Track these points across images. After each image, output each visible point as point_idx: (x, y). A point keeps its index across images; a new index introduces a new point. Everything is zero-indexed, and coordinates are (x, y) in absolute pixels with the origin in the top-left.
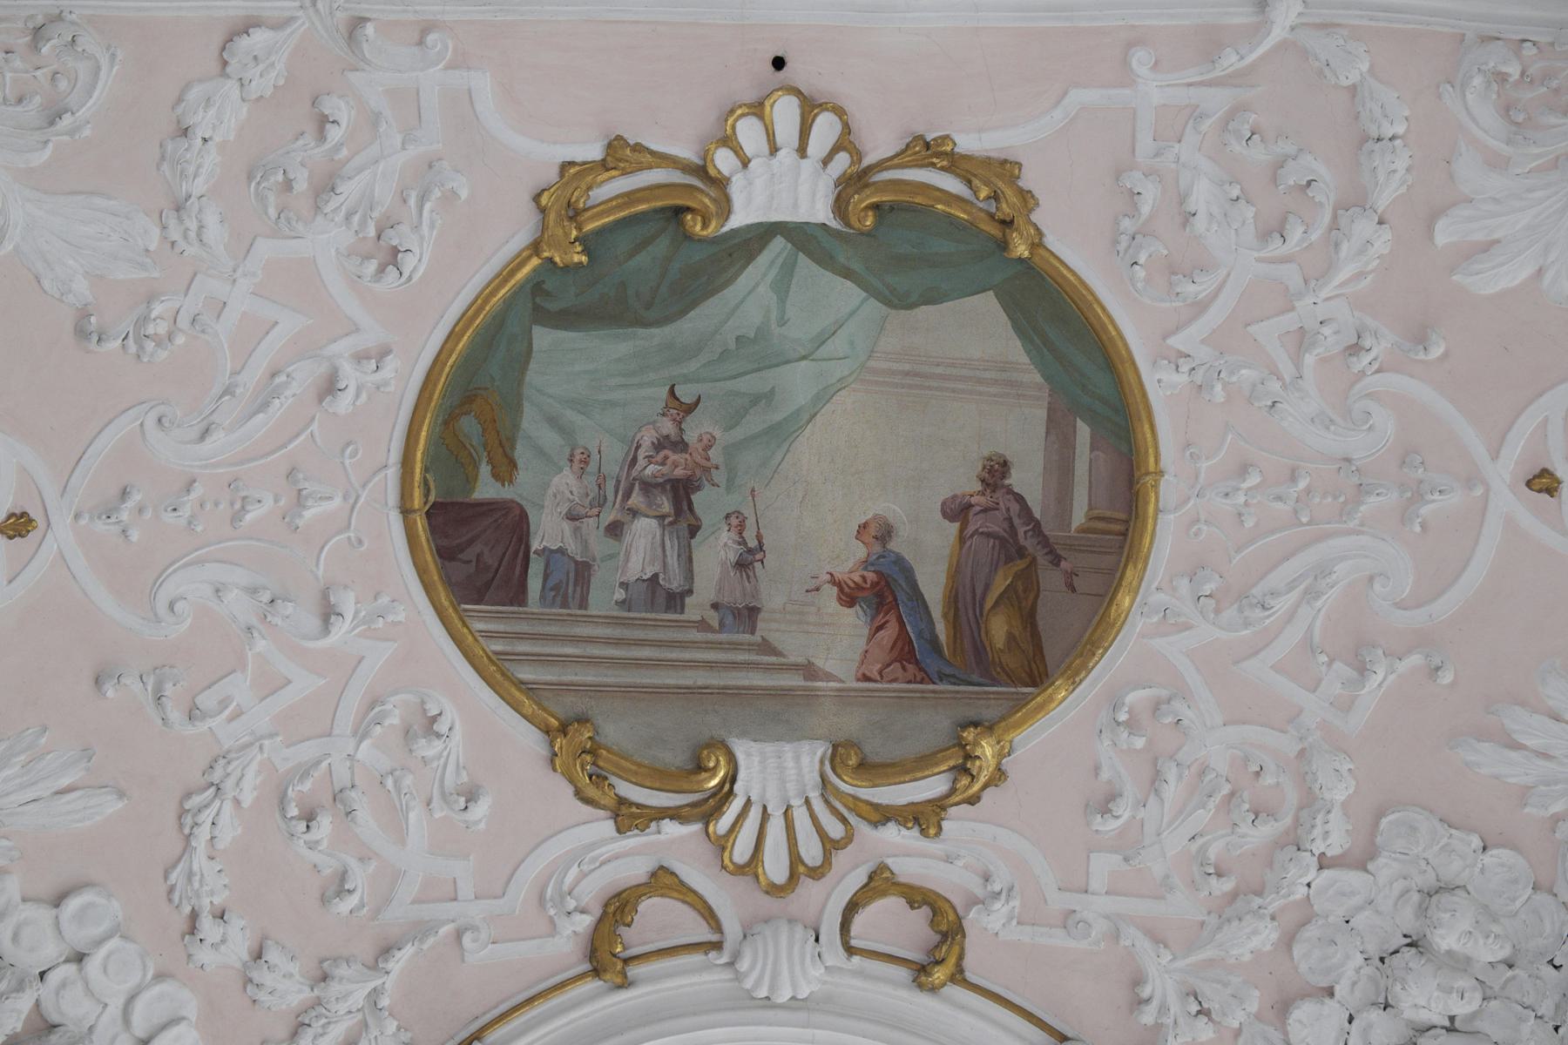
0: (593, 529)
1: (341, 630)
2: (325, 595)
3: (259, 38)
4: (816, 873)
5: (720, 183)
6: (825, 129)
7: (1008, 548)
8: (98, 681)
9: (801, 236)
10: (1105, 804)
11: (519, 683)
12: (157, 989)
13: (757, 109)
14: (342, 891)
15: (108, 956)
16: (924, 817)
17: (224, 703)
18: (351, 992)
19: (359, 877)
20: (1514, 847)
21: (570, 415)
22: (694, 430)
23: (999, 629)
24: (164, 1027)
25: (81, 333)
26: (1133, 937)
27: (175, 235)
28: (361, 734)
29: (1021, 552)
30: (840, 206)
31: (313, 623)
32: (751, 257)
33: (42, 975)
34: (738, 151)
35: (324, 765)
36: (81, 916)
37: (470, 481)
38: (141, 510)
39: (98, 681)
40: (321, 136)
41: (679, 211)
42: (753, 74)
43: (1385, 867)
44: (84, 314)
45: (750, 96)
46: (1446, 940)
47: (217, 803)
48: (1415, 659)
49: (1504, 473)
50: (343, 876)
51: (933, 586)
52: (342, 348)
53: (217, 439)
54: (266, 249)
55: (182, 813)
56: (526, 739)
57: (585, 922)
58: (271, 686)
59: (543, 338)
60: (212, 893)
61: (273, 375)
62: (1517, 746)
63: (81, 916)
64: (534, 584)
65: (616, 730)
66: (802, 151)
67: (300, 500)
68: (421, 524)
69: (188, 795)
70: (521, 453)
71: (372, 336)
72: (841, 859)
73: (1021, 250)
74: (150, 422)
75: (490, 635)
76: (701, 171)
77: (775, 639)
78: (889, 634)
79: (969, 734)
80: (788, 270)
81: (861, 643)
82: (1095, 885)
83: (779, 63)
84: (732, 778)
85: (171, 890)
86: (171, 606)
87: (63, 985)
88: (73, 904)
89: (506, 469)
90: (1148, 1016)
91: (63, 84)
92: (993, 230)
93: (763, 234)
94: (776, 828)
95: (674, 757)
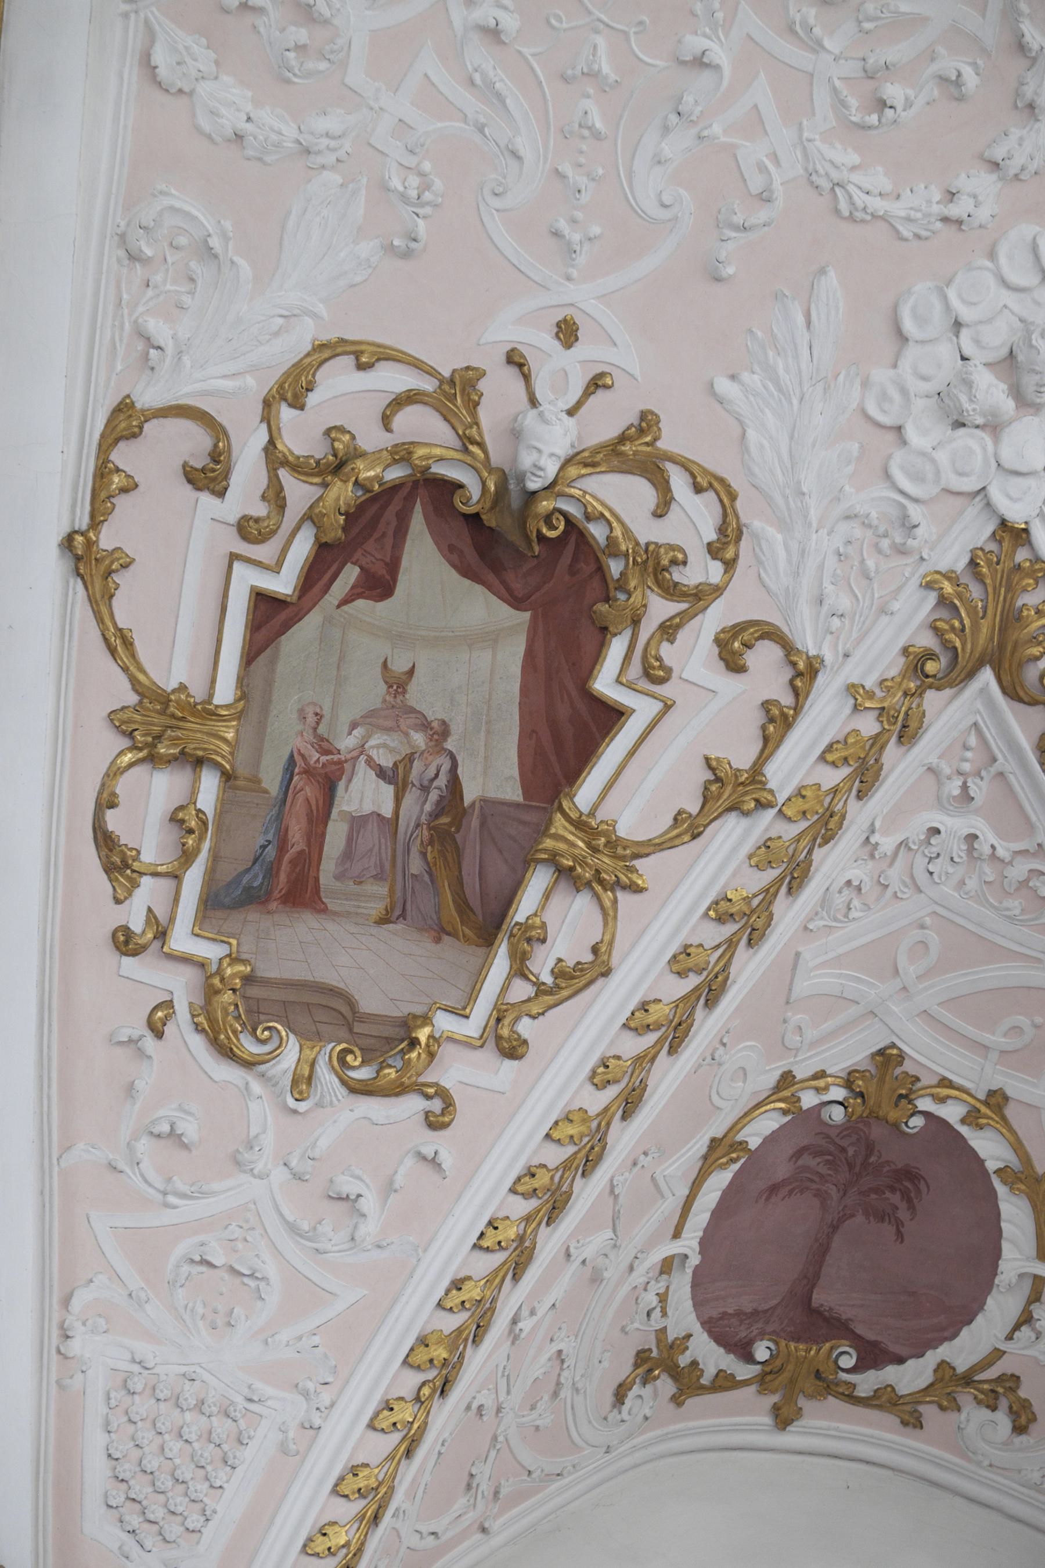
1: (719, 54)
3: (160, 57)
8: (718, 279)
12: (1003, 260)
14: (958, 82)
15: (964, 301)
17: (762, 168)
19: (948, 64)
25: (407, 254)
27: (330, 159)
28: (817, 47)
31: (706, 78)
33: (963, 358)
35: (838, 83)
36: (921, 321)
38: (574, 221)
39: (718, 279)
44: (390, 249)
47: (851, 188)
50: (943, 79)
53: (522, 145)
54: (356, 76)
55: (851, 218)
60: (929, 202)
61: (472, 83)
67: (592, 75)
69: (837, 212)
74: (496, 203)
85: (918, 236)
86: (665, 206)
87: (977, 342)
88: (909, 326)
91: (183, 241)
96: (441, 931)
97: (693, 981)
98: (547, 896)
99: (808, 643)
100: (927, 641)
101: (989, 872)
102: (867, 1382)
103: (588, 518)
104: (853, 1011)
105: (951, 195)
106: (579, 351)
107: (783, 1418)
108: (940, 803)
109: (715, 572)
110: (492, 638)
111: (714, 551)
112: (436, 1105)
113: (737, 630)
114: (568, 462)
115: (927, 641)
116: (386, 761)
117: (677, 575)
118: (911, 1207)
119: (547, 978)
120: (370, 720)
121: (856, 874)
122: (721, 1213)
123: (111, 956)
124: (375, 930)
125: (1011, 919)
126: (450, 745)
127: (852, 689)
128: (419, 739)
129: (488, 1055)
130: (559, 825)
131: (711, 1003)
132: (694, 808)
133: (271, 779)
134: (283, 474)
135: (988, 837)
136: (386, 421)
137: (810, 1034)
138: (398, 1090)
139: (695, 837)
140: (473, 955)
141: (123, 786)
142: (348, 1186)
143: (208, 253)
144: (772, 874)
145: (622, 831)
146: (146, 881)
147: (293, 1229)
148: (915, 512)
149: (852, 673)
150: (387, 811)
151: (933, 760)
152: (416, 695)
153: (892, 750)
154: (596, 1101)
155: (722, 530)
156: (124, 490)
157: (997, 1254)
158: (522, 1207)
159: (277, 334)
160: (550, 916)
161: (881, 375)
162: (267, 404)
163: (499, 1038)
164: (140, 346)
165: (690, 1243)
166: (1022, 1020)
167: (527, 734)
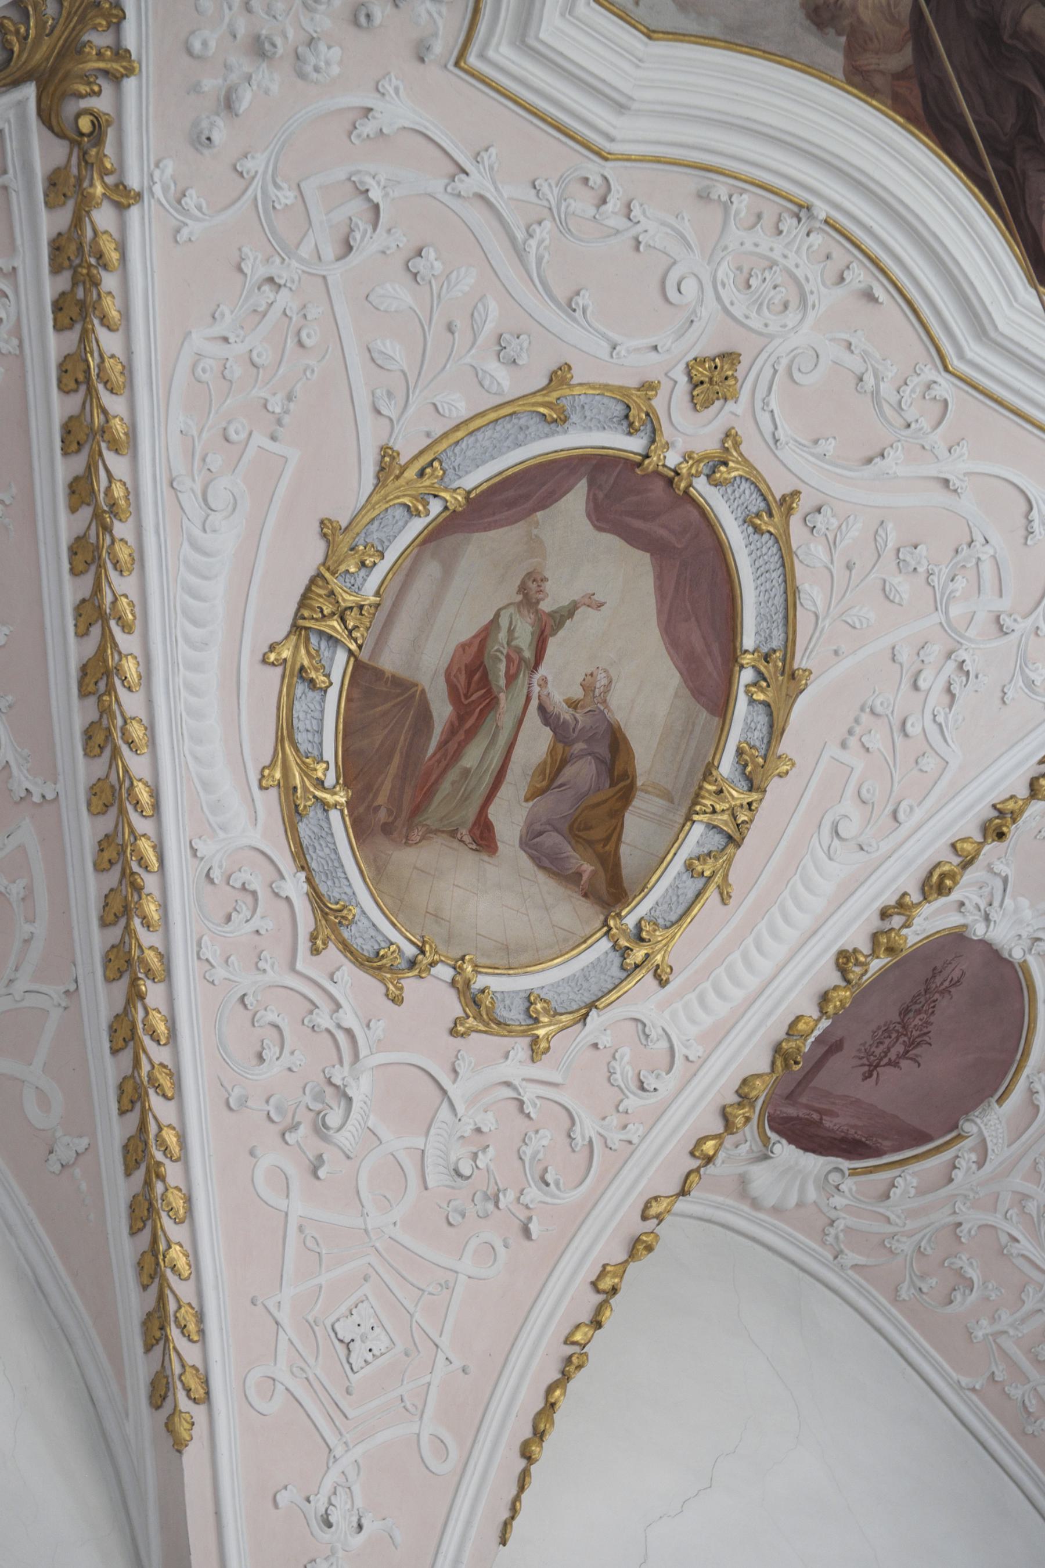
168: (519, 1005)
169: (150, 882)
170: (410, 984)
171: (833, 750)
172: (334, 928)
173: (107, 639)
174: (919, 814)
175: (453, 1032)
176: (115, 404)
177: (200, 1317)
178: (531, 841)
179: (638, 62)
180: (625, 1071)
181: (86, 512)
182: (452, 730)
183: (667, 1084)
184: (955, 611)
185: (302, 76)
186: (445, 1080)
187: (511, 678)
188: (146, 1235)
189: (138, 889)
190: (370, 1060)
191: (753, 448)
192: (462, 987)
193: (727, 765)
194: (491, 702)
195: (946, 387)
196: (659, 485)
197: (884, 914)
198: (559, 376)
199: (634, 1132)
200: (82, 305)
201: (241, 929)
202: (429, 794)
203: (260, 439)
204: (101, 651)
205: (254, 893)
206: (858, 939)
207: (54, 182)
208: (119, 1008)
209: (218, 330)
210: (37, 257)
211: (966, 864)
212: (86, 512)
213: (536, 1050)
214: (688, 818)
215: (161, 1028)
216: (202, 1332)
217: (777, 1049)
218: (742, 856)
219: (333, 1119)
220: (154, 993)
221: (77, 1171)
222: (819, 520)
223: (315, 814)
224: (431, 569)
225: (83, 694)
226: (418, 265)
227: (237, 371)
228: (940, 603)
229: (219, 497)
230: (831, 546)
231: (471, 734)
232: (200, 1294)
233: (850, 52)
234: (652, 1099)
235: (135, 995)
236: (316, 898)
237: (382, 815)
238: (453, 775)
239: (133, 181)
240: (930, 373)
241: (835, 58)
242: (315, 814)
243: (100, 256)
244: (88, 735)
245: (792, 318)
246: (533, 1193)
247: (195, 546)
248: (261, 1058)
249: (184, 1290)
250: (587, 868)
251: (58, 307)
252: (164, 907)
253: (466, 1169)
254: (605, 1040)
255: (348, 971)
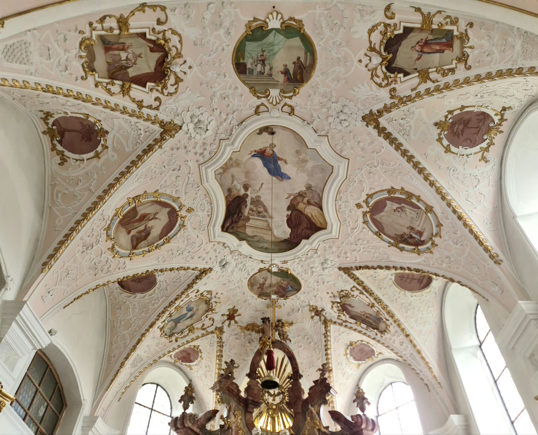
0: (254, 65)
1: (227, 78)
2: (224, 74)
3: (212, 5)
4: (279, 103)
5: (267, 23)
6: (279, 16)
7: (300, 67)
8: (201, 84)
9: (277, 30)
10: (309, 96)
11: (246, 83)
13: (271, 13)
14: (229, 106)
16: (290, 98)
17: (214, 86)
18: (230, 117)
19: (230, 105)
20: (353, 102)
21: (251, 52)
22: (265, 54)
23: (299, 77)
24: (212, 120)
25: (195, 44)
26: (312, 110)
27: (204, 31)
28: (229, 89)
29: (301, 68)
30: (281, 26)
31: (223, 77)
32: (271, 32)
34: (269, 19)
36: (202, 110)
37: (240, 60)
40: (220, 18)
41: (262, 27)
42: (270, 9)
43: (339, 103)
44: (195, 42)
45: (270, 12)
46: (345, 111)
48: (344, 81)
49: (356, 60)
50: (229, 104)
51: (291, 72)
52: (224, 45)
53: (211, 57)
54: (215, 33)
55: (211, 98)
56: (247, 89)
57: (254, 109)
58: (219, 84)
59: (247, 43)
62: (354, 91)
63: (202, 110)
64: (247, 72)
65: (257, 88)
66: (277, 19)
68: (234, 65)
70: (245, 57)
71: (227, 44)
72: (281, 102)
73: (302, 32)
75: (243, 78)
76: (265, 22)
77: (274, 78)
78: (286, 77)
79: (295, 89)
80: (275, 34)
81: (283, 78)
82: (308, 104)
83: (274, 7)
84: (270, 93)
88: (201, 109)
89: (244, 59)
90: (313, 118)
92: (298, 29)
93: (272, 29)
94: (274, 99)
95: (263, 91)
96: (109, 71)
97: (114, 107)
98: (119, 84)
99: (161, 108)
100: (165, 122)
101: (137, 138)
102: (55, 142)
103: (168, 76)
104: (112, 127)
105: (216, 109)
106: (188, 70)
107: (44, 133)
108: (144, 129)
109: (166, 94)
110: (149, 67)
111: (168, 93)
112: (85, 77)
113: (160, 99)
114: (175, 72)
115: (165, 122)
116: (129, 57)
117: (164, 90)
118: (86, 141)
119: (108, 88)
120: (134, 53)
121: (133, 123)
122: (76, 118)
123: (88, 22)
124: (106, 63)
125: (132, 142)
126: (134, 65)
127: (157, 115)
128: (133, 61)
129: (94, 83)
130: (129, 84)
131: (111, 110)
132: (136, 100)
133: (121, 41)
134: (162, 33)
135: (142, 136)
136: (173, 46)
137: (107, 122)
138: (85, 71)
139: (133, 102)
140: (107, 77)
141: (113, 18)
142: (69, 68)
143: (188, 17)
144: (131, 113)
145: (130, 92)
146: (100, 25)
147: (59, 62)
148: (180, 116)
149: (159, 114)
150: (122, 59)
151: (150, 127)
152: (139, 59)
153: (150, 122)
154: (94, 99)
155: (171, 93)
156: (154, 10)
157: (85, 153)
158: (75, 94)
159: (180, 28)
160: (116, 86)
161: (194, 107)
162: (171, 29)
163: (97, 83)
164: (174, 9)
165: (70, 115)
166: (119, 147)
167: (139, 76)
168: (116, 251)
169: (96, 210)
170: (109, 241)
171: (165, 251)
172: (108, 229)
173: (116, 183)
174: (167, 263)
175: (108, 249)
176: (140, 163)
177: (57, 259)
178: (133, 236)
179: (212, 179)
180: (119, 266)
181: (127, 170)
182: (137, 220)
183: (121, 270)
184: (187, 248)
185: (186, 153)
186: (103, 253)
187: (146, 220)
188: (59, 246)
189: (95, 209)
190: (98, 245)
191: (187, 219)
192: (113, 245)
193: (155, 244)
194: (143, 220)
195: (206, 228)
196: (176, 215)
197: (155, 270)
198: (178, 198)
199: (114, 273)
200: (147, 152)
201: (100, 222)
202: (129, 224)
203: (148, 179)
204: (115, 184)
205: (104, 220)
206: (150, 271)
207: (155, 139)
208: (80, 219)
209: (155, 166)
210: (147, 144)
211: (166, 271)
212: (127, 170)
213: (114, 257)
214: (148, 246)
215: (83, 225)
216: (56, 261)
217: (134, 275)
218: (149, 254)
219: (89, 249)
220: (85, 221)
221: (56, 232)
222: (185, 230)
223: (117, 217)
224: (150, 204)
225: (108, 186)
226: (178, 177)
227: (153, 171)
228: (187, 246)
229: (139, 180)
230: (184, 233)
231: (138, 222)
232: (59, 257)
233: (228, 195)
234: (119, 270)
235: (83, 220)
236: (109, 225)
237: (123, 222)
238: (132, 224)
239: (163, 147)
240: (206, 226)
241: (226, 195)
242: (117, 217)
243: (153, 150)
244: (105, 190)
245: (201, 211)
246: (100, 271)
247: (133, 183)
248: (89, 236)
249: (58, 255)
250: (135, 243)
251: (144, 150)
252: (95, 213)
253: (96, 264)
254: (120, 261)
255: (105, 235)
